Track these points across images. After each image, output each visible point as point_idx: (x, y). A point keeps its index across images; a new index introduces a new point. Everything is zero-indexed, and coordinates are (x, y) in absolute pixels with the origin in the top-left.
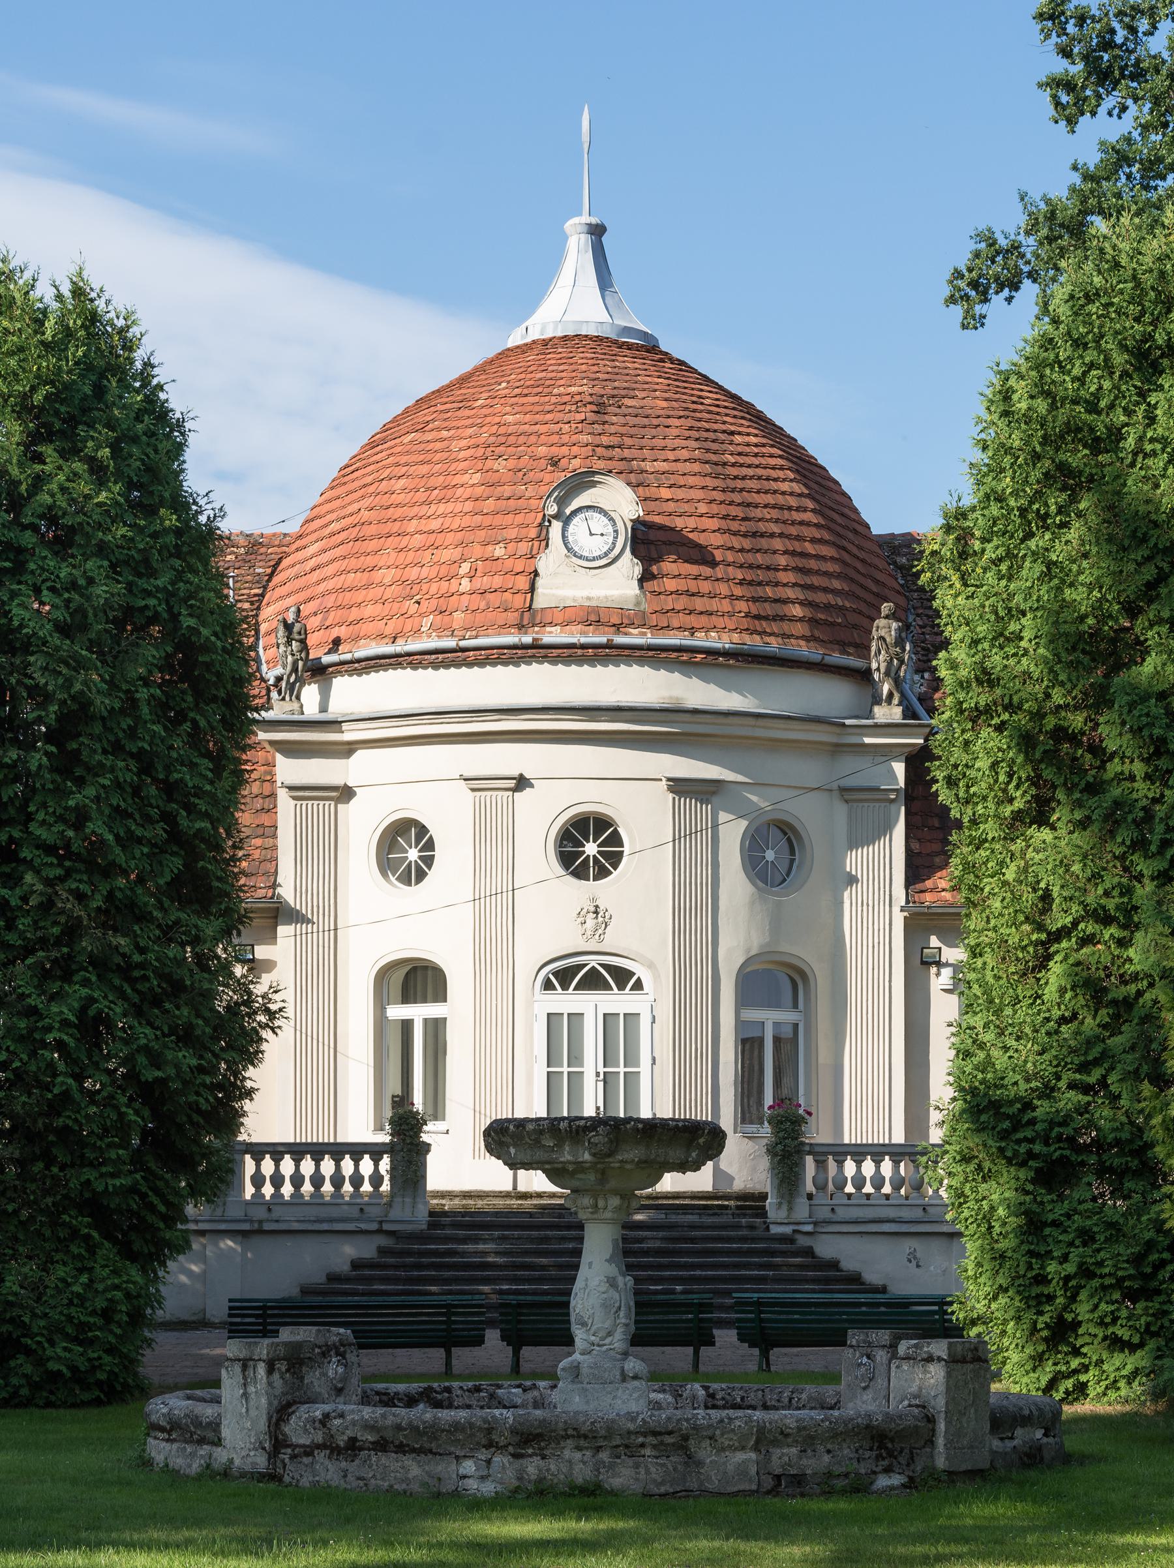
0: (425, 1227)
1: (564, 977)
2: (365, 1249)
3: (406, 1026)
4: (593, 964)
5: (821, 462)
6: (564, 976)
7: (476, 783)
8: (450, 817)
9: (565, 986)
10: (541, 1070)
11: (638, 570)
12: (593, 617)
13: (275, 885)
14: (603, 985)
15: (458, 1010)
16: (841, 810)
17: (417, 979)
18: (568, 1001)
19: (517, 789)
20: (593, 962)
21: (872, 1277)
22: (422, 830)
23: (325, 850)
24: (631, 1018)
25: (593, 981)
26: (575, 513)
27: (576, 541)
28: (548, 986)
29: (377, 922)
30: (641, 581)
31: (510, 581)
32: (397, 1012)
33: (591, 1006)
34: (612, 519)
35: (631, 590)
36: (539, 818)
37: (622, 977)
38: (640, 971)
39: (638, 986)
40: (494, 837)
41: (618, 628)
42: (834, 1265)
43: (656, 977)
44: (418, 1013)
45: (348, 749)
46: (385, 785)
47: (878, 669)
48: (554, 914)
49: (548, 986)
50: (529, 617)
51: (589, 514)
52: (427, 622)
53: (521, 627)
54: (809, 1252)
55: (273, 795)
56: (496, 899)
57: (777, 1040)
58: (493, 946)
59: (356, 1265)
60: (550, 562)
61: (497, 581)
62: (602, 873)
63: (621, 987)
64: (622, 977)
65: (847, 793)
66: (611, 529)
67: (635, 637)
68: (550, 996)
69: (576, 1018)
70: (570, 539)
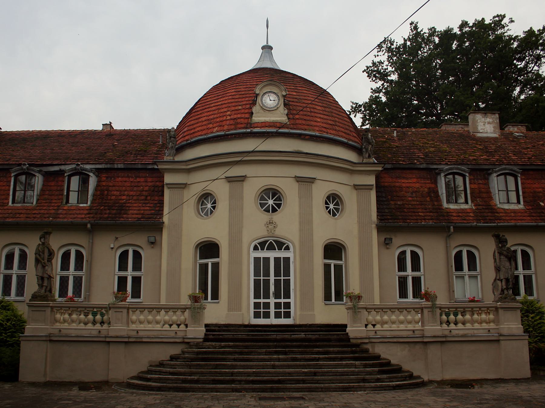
1: (262, 245)
2: (176, 350)
5: (336, 100)
6: (262, 245)
9: (262, 249)
16: (355, 192)
17: (209, 249)
18: (262, 254)
20: (271, 240)
21: (383, 356)
24: (287, 260)
25: (271, 248)
26: (265, 94)
27: (265, 102)
28: (256, 248)
33: (272, 255)
37: (281, 245)
39: (287, 248)
41: (280, 128)
42: (378, 357)
44: (210, 261)
49: (256, 248)
50: (250, 125)
54: (367, 351)
59: (172, 358)
62: (274, 210)
64: (281, 245)
65: (356, 187)
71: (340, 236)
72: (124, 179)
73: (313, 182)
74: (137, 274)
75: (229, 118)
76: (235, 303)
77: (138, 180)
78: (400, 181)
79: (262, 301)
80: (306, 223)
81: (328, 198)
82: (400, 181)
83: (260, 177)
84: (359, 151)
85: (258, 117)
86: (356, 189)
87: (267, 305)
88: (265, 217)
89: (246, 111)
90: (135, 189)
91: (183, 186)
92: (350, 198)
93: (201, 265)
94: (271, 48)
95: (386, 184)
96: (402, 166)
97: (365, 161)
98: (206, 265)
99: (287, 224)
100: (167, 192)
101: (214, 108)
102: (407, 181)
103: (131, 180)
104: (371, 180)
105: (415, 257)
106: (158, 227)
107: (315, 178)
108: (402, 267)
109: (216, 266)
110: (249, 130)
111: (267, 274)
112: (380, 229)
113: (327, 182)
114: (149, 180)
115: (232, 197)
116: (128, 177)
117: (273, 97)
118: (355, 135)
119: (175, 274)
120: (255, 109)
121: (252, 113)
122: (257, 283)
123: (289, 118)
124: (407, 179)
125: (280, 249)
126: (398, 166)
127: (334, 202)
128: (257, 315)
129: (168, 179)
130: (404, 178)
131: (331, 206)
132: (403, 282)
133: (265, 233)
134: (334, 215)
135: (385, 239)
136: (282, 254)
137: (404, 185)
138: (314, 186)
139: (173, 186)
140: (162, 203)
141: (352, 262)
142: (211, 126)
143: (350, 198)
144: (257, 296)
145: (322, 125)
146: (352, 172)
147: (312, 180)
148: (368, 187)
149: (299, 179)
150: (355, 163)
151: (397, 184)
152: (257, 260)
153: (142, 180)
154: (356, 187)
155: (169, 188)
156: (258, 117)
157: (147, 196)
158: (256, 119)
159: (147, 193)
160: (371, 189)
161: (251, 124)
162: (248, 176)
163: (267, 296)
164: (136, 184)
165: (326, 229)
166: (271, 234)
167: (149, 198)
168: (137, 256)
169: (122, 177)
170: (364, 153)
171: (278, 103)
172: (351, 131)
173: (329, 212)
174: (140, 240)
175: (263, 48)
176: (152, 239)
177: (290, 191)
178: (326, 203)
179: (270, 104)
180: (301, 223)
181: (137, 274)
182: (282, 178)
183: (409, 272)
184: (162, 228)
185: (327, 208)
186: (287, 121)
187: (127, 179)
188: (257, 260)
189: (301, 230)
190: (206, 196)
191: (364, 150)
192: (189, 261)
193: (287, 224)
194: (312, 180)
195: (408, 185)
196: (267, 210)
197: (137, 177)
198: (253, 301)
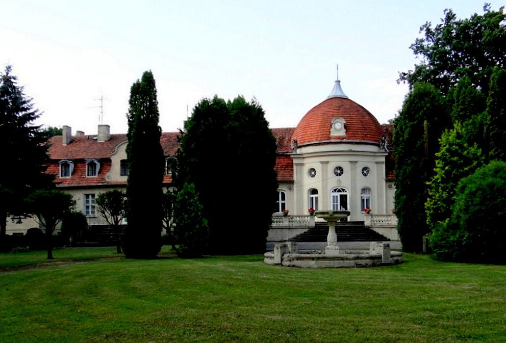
3: (313, 198)
7: (322, 163)
8: (318, 167)
10: (332, 204)
11: (345, 131)
12: (339, 138)
13: (293, 178)
15: (319, 195)
16: (376, 165)
17: (314, 191)
20: (339, 188)
22: (314, 170)
23: (301, 173)
25: (339, 191)
26: (336, 123)
29: (309, 183)
30: (346, 132)
31: (326, 133)
32: (312, 196)
35: (345, 134)
36: (331, 168)
37: (344, 190)
38: (346, 190)
39: (346, 191)
40: (324, 171)
41: (342, 139)
44: (314, 196)
45: (304, 158)
46: (309, 163)
48: (333, 181)
49: (333, 192)
50: (329, 138)
52: (314, 140)
53: (328, 140)
55: (293, 165)
56: (325, 180)
57: (367, 200)
58: (324, 188)
60: (332, 130)
61: (325, 133)
62: (340, 175)
64: (344, 190)
65: (377, 163)
67: (345, 140)
69: (337, 196)
71: (369, 186)
74: (283, 202)
75: (320, 134)
77: (281, 160)
80: (353, 180)
81: (364, 168)
83: (335, 162)
84: (378, 145)
85: (334, 134)
89: (328, 131)
90: (280, 164)
92: (373, 168)
93: (310, 198)
94: (339, 82)
97: (381, 151)
98: (313, 198)
99: (345, 181)
100: (295, 167)
101: (313, 128)
104: (383, 159)
106: (292, 182)
109: (317, 198)
110: (329, 141)
111: (337, 202)
112: (387, 181)
113: (363, 162)
114: (286, 160)
115: (323, 170)
117: (339, 124)
119: (300, 201)
121: (330, 132)
122: (334, 205)
123: (346, 134)
125: (343, 191)
127: (365, 171)
129: (295, 161)
131: (365, 172)
134: (366, 175)
136: (343, 193)
139: (297, 164)
140: (292, 170)
142: (312, 137)
143: (373, 168)
147: (356, 162)
148: (382, 163)
149: (351, 162)
152: (334, 196)
153: (282, 160)
154: (377, 163)
156: (334, 134)
161: (330, 137)
165: (362, 182)
173: (364, 175)
175: (336, 82)
176: (289, 188)
178: (363, 170)
179: (338, 128)
181: (283, 202)
182: (343, 162)
185: (363, 173)
188: (334, 196)
190: (313, 170)
192: (306, 196)
193: (345, 181)
194: (356, 162)
197: (280, 159)
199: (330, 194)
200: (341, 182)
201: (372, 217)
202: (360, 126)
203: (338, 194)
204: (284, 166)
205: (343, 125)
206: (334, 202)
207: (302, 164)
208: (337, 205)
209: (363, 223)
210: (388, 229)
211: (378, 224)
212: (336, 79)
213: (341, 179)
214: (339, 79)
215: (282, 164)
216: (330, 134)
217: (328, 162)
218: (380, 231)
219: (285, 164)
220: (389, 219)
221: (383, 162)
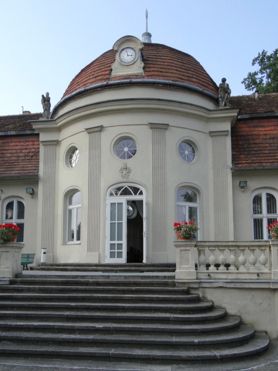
0: (7, 283)
4: (126, 186)
5: (198, 61)
7: (90, 131)
10: (108, 222)
11: (143, 65)
14: (130, 194)
16: (210, 140)
19: (100, 131)
20: (126, 185)
23: (53, 160)
25: (126, 192)
27: (123, 58)
28: (111, 194)
30: (144, 68)
34: (135, 51)
35: (141, 71)
36: (107, 139)
37: (136, 190)
39: (141, 193)
40: (94, 148)
43: (147, 190)
47: (221, 97)
51: (127, 50)
61: (100, 73)
63: (135, 194)
64: (136, 190)
65: (212, 134)
66: (134, 54)
68: (112, 198)
69: (120, 204)
70: (122, 58)
72: (16, 144)
73: (166, 129)
76: (92, 247)
77: (27, 143)
78: (257, 129)
79: (116, 242)
80: (159, 168)
82: (257, 129)
83: (116, 126)
86: (212, 136)
87: (120, 246)
88: (120, 163)
90: (24, 151)
91: (55, 143)
92: (206, 145)
95: (244, 133)
96: (259, 115)
100: (42, 149)
102: (264, 129)
103: (22, 144)
104: (227, 127)
105: (271, 200)
107: (168, 125)
108: (257, 210)
112: (237, 173)
116: (20, 142)
118: (213, 88)
120: (114, 66)
122: (112, 225)
123: (145, 71)
124: (264, 127)
126: (255, 115)
128: (112, 255)
130: (261, 126)
132: (258, 223)
133: (120, 179)
134: (189, 160)
135: (240, 182)
136: (134, 197)
137: (261, 133)
138: (167, 133)
139: (47, 143)
141: (206, 206)
143: (206, 145)
144: (112, 238)
145: (178, 76)
146: (208, 120)
147: (165, 127)
148: (222, 133)
149: (153, 126)
150: (210, 110)
151: (254, 133)
152: (113, 205)
154: (212, 134)
155: (44, 145)
157: (32, 157)
158: (114, 74)
159: (33, 153)
160: (227, 135)
162: (104, 126)
163: (120, 238)
164: (25, 147)
165: (178, 173)
166: (125, 180)
167: (34, 157)
168: (21, 206)
169: (15, 142)
170: (220, 103)
171: (135, 58)
172: (208, 84)
174: (21, 193)
177: (143, 137)
180: (153, 168)
182: (136, 126)
183: (265, 215)
184: (38, 181)
186: (143, 73)
187: (18, 144)
188: (113, 205)
189: (154, 175)
191: (220, 99)
193: (141, 171)
194: (165, 127)
195: (265, 133)
196: (123, 157)
197: (26, 142)
198: (108, 242)
199: (105, 200)
200: (129, 172)
201: (199, 252)
202: (179, 63)
203: (123, 199)
204: (31, 154)
205: (139, 54)
206: (112, 218)
207: (57, 143)
208: (120, 225)
209: (172, 267)
210: (259, 297)
211: (221, 275)
212: (145, 31)
213: (128, 166)
214: (149, 31)
215: (27, 151)
216: (110, 74)
217: (101, 128)
218: (231, 303)
219: (33, 150)
220: (262, 258)
221: (228, 131)
